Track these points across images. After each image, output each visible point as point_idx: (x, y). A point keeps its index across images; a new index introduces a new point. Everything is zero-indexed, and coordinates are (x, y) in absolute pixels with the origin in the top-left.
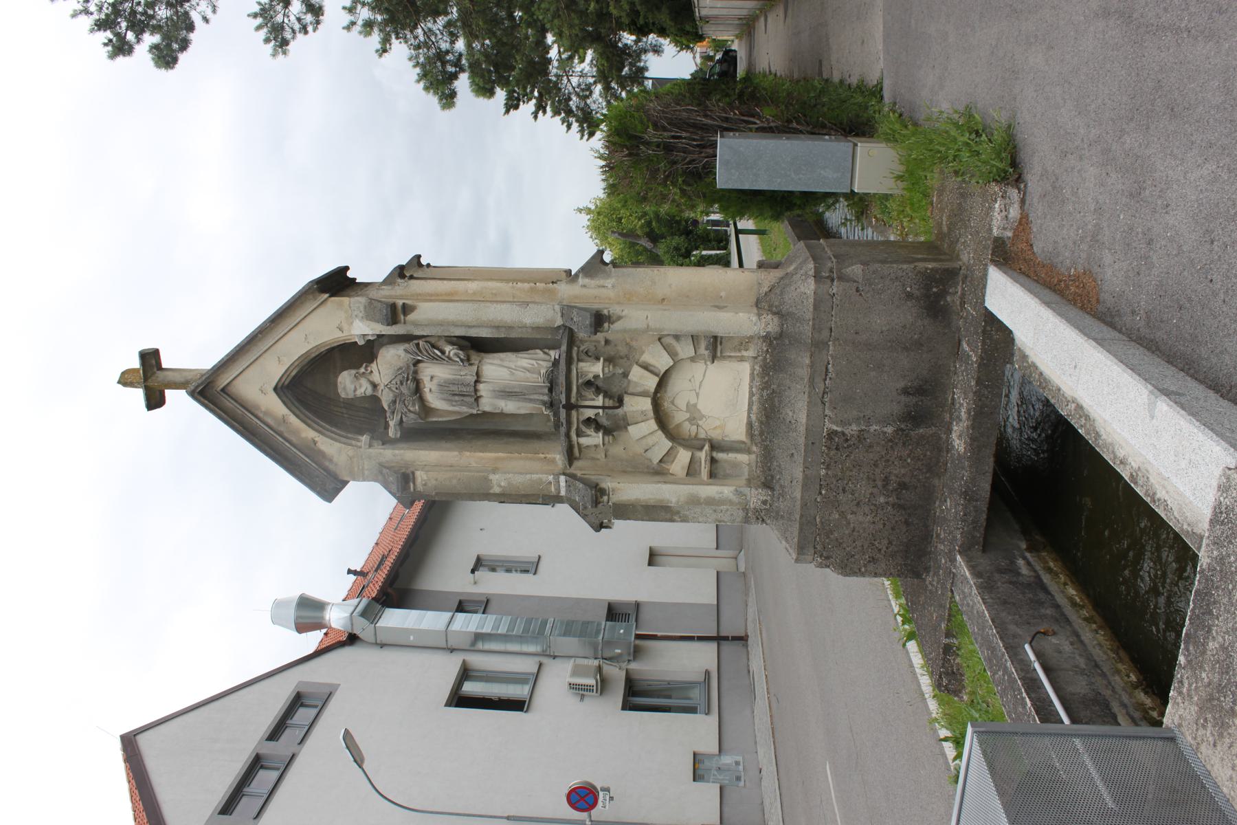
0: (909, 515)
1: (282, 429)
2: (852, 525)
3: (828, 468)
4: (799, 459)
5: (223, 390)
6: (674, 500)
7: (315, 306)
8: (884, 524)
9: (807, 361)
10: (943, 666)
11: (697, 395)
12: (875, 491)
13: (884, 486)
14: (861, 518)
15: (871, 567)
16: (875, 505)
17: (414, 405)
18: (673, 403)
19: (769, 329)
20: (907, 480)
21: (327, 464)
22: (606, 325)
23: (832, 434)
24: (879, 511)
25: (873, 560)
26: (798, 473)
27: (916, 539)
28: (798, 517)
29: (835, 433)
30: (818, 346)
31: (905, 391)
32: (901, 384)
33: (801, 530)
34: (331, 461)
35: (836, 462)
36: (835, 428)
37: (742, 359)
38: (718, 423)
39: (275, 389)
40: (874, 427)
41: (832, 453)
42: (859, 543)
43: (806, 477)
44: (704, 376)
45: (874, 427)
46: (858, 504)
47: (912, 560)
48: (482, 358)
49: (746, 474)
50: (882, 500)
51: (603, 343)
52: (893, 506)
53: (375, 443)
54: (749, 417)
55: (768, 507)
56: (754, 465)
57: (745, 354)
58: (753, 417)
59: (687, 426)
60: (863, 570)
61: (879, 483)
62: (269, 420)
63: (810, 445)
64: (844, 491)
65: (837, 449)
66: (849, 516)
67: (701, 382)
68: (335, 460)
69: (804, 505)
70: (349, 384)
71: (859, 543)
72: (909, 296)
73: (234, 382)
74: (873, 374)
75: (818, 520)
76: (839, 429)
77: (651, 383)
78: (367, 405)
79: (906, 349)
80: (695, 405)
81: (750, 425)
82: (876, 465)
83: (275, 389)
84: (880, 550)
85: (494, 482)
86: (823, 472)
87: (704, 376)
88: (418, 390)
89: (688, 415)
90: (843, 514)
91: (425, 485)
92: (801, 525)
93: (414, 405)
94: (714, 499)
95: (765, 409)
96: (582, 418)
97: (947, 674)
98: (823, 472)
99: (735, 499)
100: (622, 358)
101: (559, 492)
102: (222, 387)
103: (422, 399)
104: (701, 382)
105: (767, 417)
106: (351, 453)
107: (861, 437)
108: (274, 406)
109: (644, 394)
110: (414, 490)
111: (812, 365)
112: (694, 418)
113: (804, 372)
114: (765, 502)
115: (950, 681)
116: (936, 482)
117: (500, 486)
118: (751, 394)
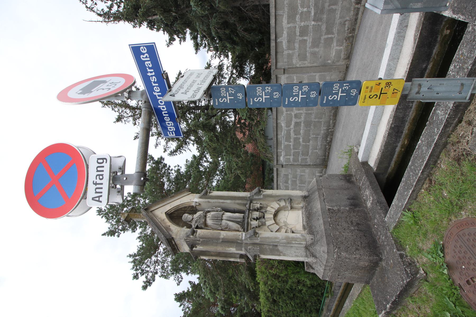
0: (364, 233)
1: (162, 222)
2: (345, 236)
3: (331, 218)
4: (321, 218)
5: (151, 212)
6: (281, 237)
8: (357, 237)
9: (317, 193)
10: (404, 265)
11: (287, 219)
12: (349, 225)
14: (347, 234)
15: (357, 252)
17: (203, 219)
19: (305, 194)
20: (359, 222)
21: (170, 232)
23: (329, 209)
24: (353, 232)
25: (357, 249)
26: (321, 221)
27: (371, 242)
28: (324, 234)
29: (330, 209)
30: (319, 189)
31: (348, 199)
32: (347, 197)
33: (326, 238)
34: (172, 231)
36: (330, 208)
37: (298, 209)
38: (293, 226)
39: (166, 213)
40: (342, 208)
41: (331, 214)
42: (349, 243)
43: (324, 221)
45: (342, 208)
46: (344, 229)
47: (373, 250)
50: (353, 228)
52: (357, 230)
54: (303, 224)
58: (304, 223)
60: (355, 253)
62: (159, 220)
63: (323, 213)
64: (338, 225)
65: (332, 213)
66: (343, 233)
68: (173, 231)
69: (326, 230)
70: (186, 217)
71: (349, 243)
72: (341, 179)
74: (337, 195)
75: (332, 234)
76: (331, 208)
79: (345, 190)
80: (286, 222)
81: (304, 226)
82: (347, 218)
83: (166, 213)
84: (358, 246)
85: (222, 234)
86: (329, 220)
88: (205, 216)
89: (284, 224)
90: (340, 232)
92: (326, 236)
93: (203, 219)
94: (294, 237)
95: (307, 217)
96: (252, 217)
97: (407, 266)
98: (329, 220)
99: (301, 237)
101: (242, 238)
103: (205, 220)
105: (308, 218)
106: (179, 230)
107: (339, 210)
108: (164, 217)
109: (271, 214)
111: (319, 193)
112: (286, 225)
113: (317, 196)
114: (312, 239)
115: (410, 268)
116: (369, 223)
118: (303, 218)
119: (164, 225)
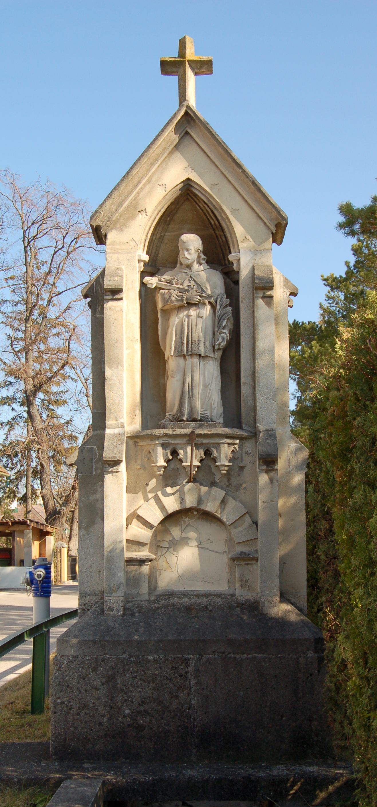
5: (187, 133)
7: (266, 221)
12: (135, 705)
13: (139, 712)
16: (122, 706)
18: (189, 525)
22: (265, 467)
35: (160, 668)
39: (188, 179)
44: (214, 551)
48: (217, 361)
49: (130, 592)
51: (241, 465)
53: (142, 264)
55: (106, 612)
56: (138, 599)
57: (238, 585)
59: (168, 538)
61: (142, 708)
67: (207, 549)
73: (195, 145)
77: (210, 507)
78: (160, 255)
87: (214, 551)
91: (110, 309)
100: (228, 481)
101: (109, 428)
102: (190, 132)
103: (180, 308)
104: (207, 549)
110: (106, 299)
117: (112, 376)
119: (142, 194)
